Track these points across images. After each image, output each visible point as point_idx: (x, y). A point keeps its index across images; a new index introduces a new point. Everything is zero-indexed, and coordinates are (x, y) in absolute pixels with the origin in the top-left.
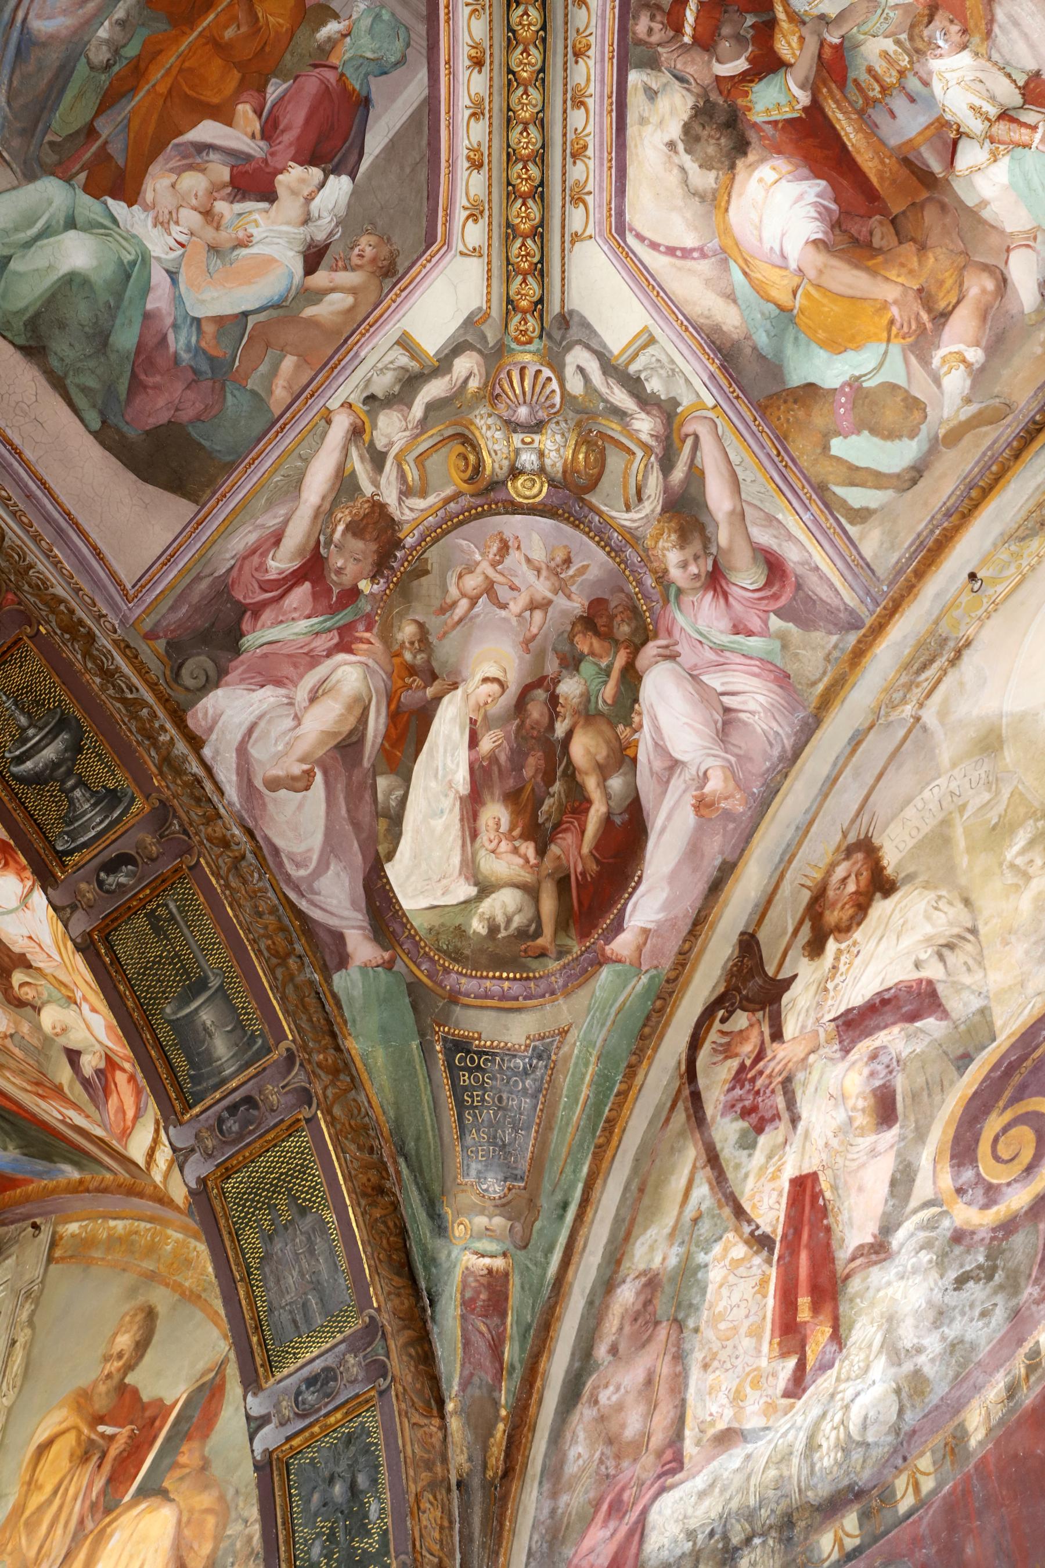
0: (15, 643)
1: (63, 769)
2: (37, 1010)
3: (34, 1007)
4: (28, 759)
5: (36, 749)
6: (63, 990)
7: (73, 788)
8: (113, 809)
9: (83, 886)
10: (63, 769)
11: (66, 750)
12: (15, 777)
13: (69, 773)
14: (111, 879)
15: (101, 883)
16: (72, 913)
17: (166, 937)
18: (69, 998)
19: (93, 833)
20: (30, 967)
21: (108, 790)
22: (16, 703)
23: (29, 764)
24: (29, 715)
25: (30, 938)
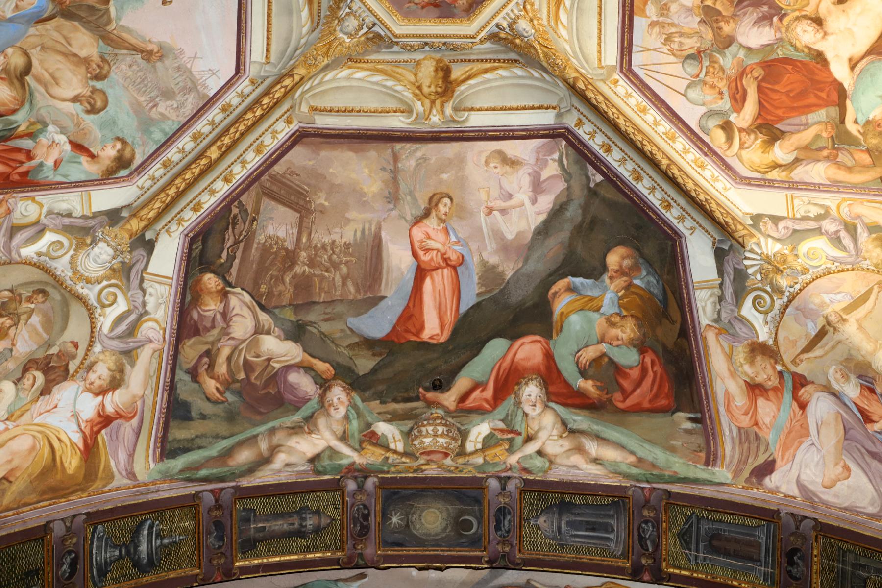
0: (200, 564)
1: (132, 550)
2: (17, 382)
3: (19, 380)
4: (148, 534)
5: (150, 541)
6: (18, 413)
7: (120, 552)
8: (98, 570)
9: (75, 540)
10: (132, 550)
11: (139, 557)
12: (146, 520)
13: (128, 553)
14: (68, 560)
15: (69, 552)
16: (66, 527)
17: (22, 579)
18: (12, 415)
19: (94, 552)
20: (41, 394)
21: (108, 572)
22: (175, 542)
23: (146, 532)
24: (166, 546)
25: (56, 407)
